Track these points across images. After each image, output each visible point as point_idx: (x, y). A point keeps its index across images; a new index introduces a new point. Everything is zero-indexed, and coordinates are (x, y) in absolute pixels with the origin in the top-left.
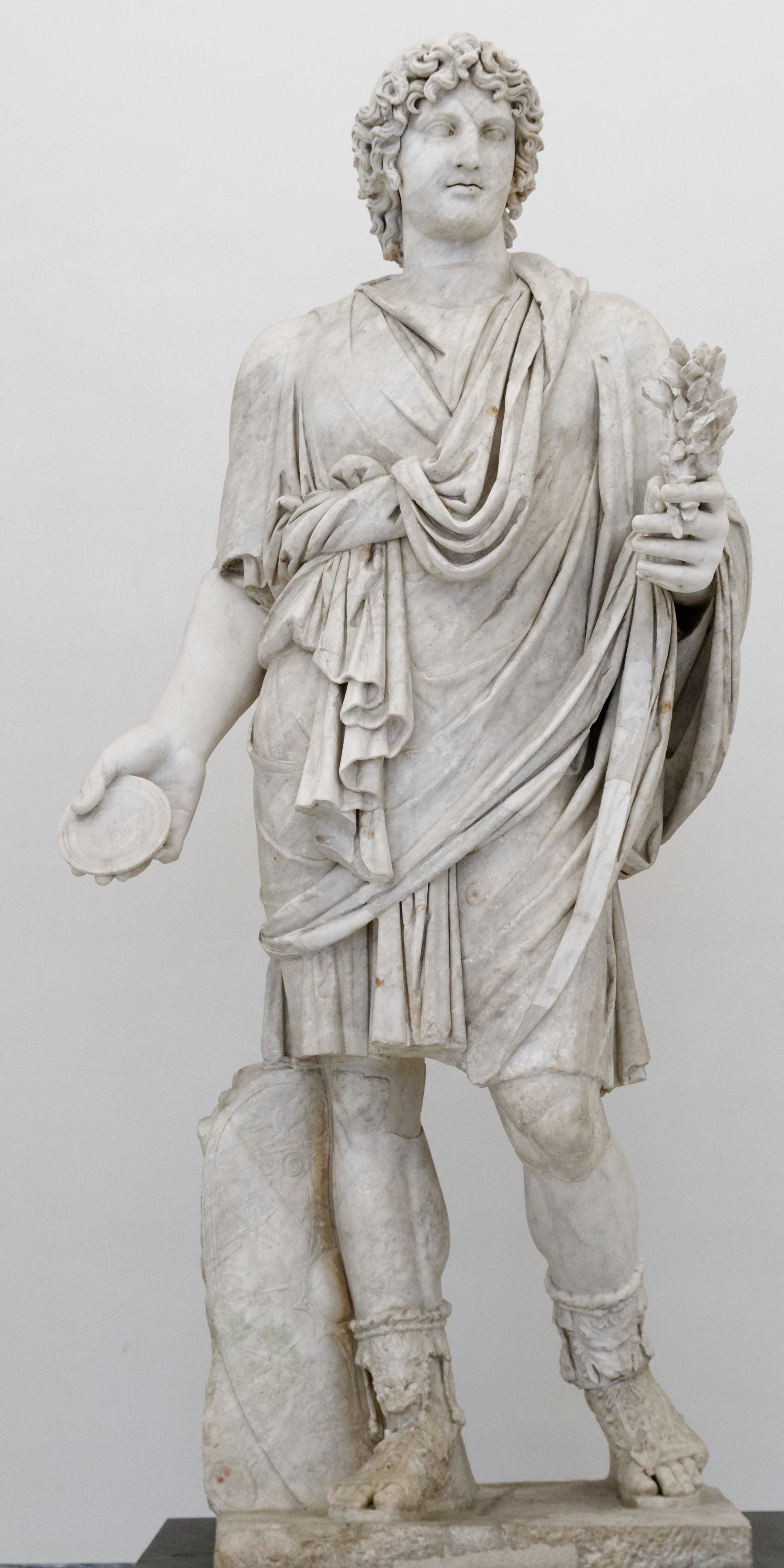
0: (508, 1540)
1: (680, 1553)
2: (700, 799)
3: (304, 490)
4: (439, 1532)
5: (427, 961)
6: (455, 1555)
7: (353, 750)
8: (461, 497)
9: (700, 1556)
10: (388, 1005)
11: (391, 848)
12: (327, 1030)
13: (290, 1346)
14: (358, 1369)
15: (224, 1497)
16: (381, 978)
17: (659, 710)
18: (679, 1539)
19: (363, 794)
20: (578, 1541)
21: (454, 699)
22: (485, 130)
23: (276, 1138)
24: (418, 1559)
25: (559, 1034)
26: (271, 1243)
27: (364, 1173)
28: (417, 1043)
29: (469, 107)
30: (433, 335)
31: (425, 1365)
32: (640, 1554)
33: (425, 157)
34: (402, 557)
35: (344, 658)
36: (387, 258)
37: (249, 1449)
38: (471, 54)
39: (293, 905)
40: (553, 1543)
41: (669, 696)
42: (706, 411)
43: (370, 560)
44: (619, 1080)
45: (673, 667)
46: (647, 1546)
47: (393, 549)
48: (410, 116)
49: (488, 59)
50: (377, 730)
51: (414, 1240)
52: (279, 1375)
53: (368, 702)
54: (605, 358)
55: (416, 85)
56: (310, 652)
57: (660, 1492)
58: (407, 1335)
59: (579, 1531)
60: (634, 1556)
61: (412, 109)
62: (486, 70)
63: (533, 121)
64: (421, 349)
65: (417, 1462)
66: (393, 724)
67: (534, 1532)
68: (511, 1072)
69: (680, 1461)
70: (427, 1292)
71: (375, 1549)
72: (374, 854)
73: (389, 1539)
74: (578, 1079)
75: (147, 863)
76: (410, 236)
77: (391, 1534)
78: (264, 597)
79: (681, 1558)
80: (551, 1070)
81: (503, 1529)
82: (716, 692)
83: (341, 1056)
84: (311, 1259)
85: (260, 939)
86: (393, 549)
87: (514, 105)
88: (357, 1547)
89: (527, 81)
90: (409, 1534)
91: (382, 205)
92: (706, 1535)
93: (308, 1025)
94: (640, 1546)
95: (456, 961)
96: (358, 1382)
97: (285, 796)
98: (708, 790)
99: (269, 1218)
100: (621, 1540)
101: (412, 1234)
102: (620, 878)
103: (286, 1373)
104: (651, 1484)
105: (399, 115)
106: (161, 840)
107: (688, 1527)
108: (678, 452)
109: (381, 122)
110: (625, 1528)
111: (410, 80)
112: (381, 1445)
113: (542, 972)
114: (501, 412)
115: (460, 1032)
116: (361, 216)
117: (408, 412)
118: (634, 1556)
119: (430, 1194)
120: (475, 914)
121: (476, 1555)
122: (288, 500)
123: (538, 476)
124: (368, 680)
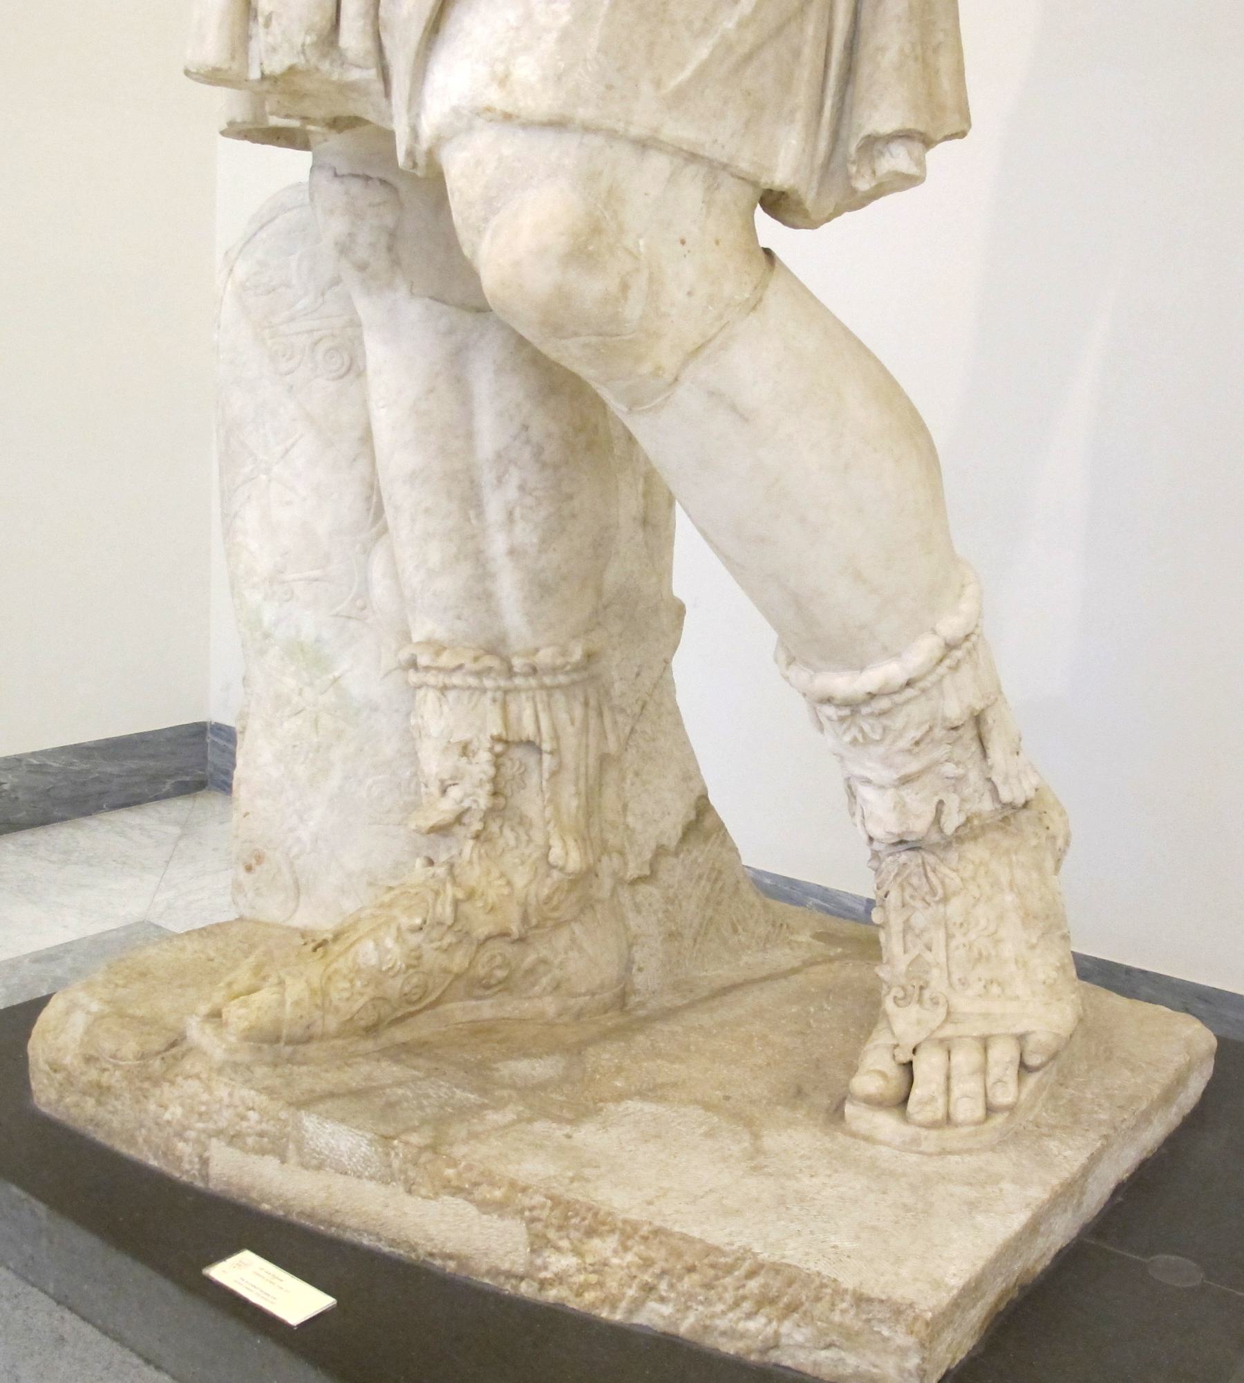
0: (401, 1171)
1: (750, 1316)
4: (283, 1115)
6: (305, 1166)
9: (799, 1337)
13: (331, 677)
15: (250, 895)
18: (753, 1285)
20: (533, 1220)
23: (299, 306)
24: (245, 1150)
31: (484, 756)
32: (663, 1286)
37: (292, 830)
40: (485, 1206)
46: (680, 1278)
51: (480, 514)
52: (316, 721)
58: (451, 695)
59: (538, 1199)
65: (389, 942)
67: (450, 1172)
71: (182, 1105)
73: (205, 1097)
74: (570, 142)
77: (208, 1089)
79: (752, 1325)
81: (394, 1148)
84: (374, 530)
88: (157, 1092)
90: (237, 1101)
92: (818, 1299)
94: (664, 1272)
99: (287, 451)
100: (626, 1249)
101: (472, 501)
107: (776, 1269)
110: (635, 1226)
118: (649, 1289)
119: (526, 428)
121: (341, 1179)
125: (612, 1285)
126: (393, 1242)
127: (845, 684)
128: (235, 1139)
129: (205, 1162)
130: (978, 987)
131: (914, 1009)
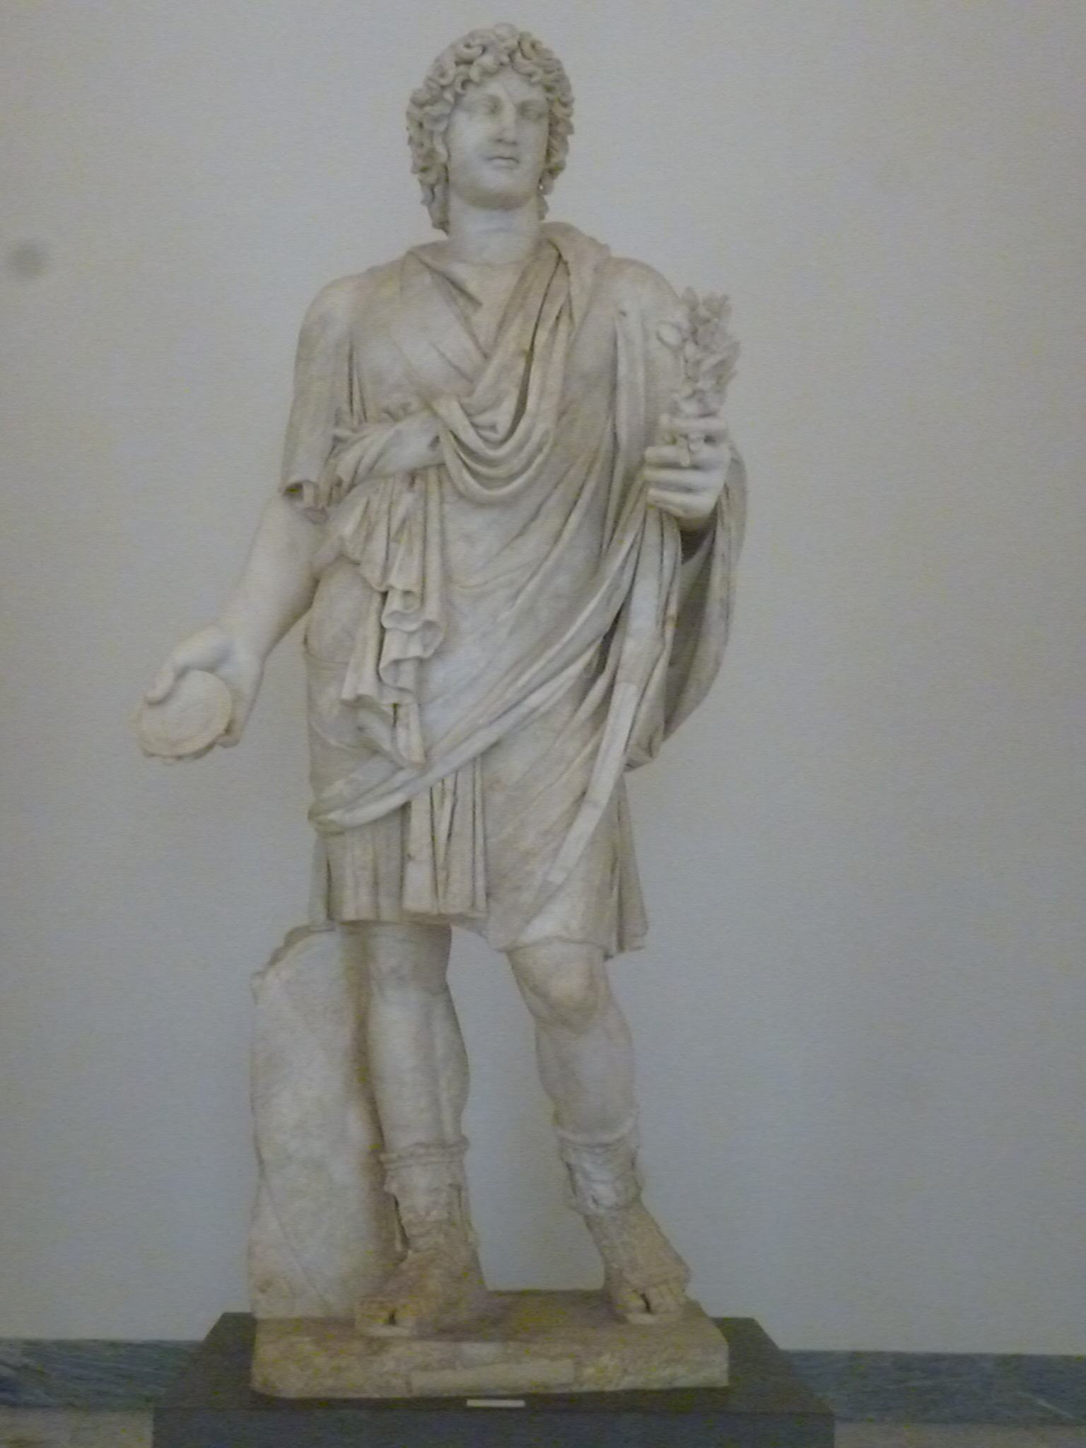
2: (698, 703)
3: (356, 422)
5: (453, 839)
7: (393, 650)
8: (493, 428)
10: (418, 875)
11: (424, 739)
12: (365, 898)
14: (386, 1194)
16: (412, 854)
17: (664, 623)
19: (401, 690)
22: (523, 109)
26: (310, 1086)
27: (398, 1023)
28: (443, 911)
29: (510, 89)
30: (472, 287)
33: (471, 132)
34: (440, 483)
35: (386, 570)
36: (435, 226)
38: (512, 43)
39: (339, 787)
41: (673, 610)
42: (713, 353)
43: (412, 483)
44: (621, 947)
45: (676, 587)
47: (432, 476)
48: (457, 97)
49: (526, 47)
50: (412, 634)
53: (406, 608)
54: (623, 314)
55: (462, 68)
56: (357, 564)
57: (648, 1308)
61: (459, 89)
62: (524, 56)
63: (565, 105)
64: (462, 301)
69: (666, 1282)
70: (449, 1129)
72: (409, 741)
75: (210, 747)
76: (456, 203)
78: (319, 516)
82: (714, 609)
83: (377, 922)
85: (309, 818)
86: (432, 476)
87: (549, 89)
89: (560, 69)
91: (431, 177)
93: (348, 893)
95: (480, 841)
96: (386, 1206)
97: (332, 691)
98: (705, 695)
102: (625, 770)
104: (641, 1303)
105: (448, 96)
106: (221, 727)
108: (687, 390)
109: (433, 101)
111: (457, 64)
112: (404, 1266)
113: (556, 851)
114: (530, 355)
115: (481, 902)
116: (413, 188)
117: (449, 355)
120: (498, 798)
122: (343, 432)
123: (562, 414)
124: (408, 588)
128: (426, 1368)
129: (408, 1383)
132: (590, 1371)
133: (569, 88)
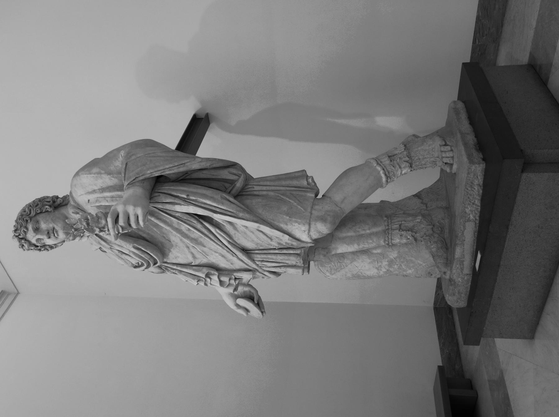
18: (469, 189)
19: (230, 280)
21: (198, 255)
25: (297, 230)
31: (402, 233)
40: (465, 229)
54: (89, 201)
60: (473, 204)
66: (208, 275)
68: (310, 241)
74: (312, 223)
80: (309, 233)
101: (362, 236)
103: (402, 260)
125: (474, 209)
126: (474, 243)
127: (384, 179)
128: (462, 269)
129: (467, 274)
130: (433, 153)
131: (437, 163)
132: (472, 217)
133: (24, 210)
